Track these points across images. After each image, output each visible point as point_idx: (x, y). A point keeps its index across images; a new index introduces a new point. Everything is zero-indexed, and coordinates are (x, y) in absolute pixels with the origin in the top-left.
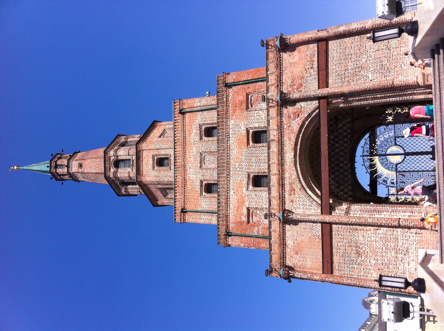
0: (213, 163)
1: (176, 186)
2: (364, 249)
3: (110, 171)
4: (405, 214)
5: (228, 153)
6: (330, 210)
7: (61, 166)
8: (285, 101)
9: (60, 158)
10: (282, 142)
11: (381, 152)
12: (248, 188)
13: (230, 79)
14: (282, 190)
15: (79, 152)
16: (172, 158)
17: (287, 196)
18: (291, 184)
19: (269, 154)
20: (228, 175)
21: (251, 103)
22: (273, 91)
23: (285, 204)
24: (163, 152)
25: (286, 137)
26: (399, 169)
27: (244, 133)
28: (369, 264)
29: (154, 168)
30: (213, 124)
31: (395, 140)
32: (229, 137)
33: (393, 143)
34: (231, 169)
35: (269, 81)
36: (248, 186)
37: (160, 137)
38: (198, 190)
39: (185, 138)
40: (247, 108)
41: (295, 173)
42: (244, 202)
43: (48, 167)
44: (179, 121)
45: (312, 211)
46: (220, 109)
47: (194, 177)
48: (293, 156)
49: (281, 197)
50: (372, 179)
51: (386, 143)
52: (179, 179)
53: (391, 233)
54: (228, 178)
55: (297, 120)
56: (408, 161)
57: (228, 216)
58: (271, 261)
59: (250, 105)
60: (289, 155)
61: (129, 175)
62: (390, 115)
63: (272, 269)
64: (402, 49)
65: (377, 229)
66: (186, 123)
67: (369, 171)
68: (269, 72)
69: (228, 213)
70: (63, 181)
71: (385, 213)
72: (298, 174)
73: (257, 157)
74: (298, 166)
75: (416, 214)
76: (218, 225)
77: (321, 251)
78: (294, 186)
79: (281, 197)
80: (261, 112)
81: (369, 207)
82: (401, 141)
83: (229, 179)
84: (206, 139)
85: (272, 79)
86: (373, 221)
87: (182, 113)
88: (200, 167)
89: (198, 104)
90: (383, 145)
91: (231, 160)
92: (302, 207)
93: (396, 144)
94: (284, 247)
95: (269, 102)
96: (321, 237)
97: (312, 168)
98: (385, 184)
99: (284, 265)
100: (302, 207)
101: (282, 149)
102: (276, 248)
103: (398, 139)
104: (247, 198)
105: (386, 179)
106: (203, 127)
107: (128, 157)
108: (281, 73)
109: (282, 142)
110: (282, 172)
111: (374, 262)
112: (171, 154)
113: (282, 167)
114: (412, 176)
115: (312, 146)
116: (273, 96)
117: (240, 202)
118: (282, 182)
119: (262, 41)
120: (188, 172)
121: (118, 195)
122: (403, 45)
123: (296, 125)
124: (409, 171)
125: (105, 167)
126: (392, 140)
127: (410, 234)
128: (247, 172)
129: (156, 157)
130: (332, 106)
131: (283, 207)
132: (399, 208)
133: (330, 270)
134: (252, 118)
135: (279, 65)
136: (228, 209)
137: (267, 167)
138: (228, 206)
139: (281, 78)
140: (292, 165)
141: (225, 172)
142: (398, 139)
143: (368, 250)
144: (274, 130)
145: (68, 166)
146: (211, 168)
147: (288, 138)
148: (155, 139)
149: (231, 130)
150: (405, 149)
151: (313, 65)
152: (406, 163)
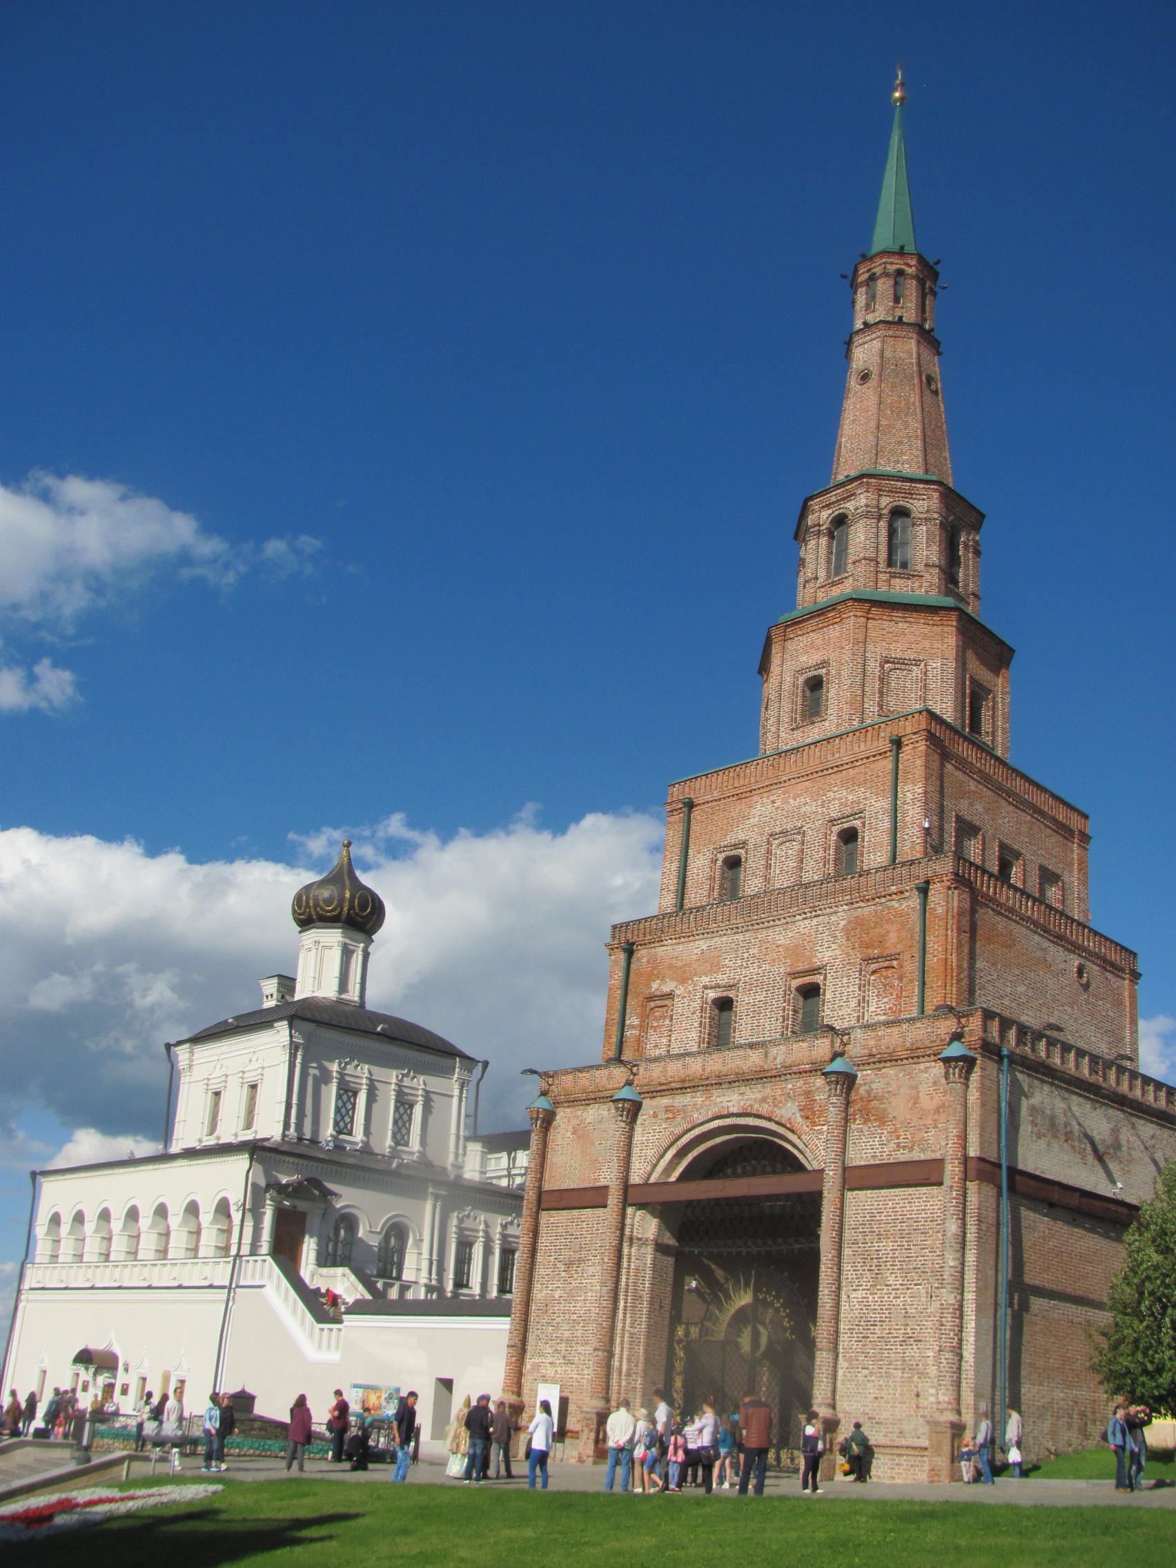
4: (625, 1361)
17: (665, 1101)
18: (684, 1110)
29: (800, 672)
38: (730, 839)
39: (839, 768)
40: (868, 960)
42: (683, 981)
58: (566, 1072)
60: (731, 1100)
64: (899, 1372)
66: (873, 766)
71: (628, 1321)
80: (853, 1003)
96: (598, 1184)
106: (857, 823)
111: (557, 1296)
112: (827, 723)
123: (790, 1111)
135: (915, 1054)
140: (715, 1110)
146: (768, 867)
151: (904, 1148)
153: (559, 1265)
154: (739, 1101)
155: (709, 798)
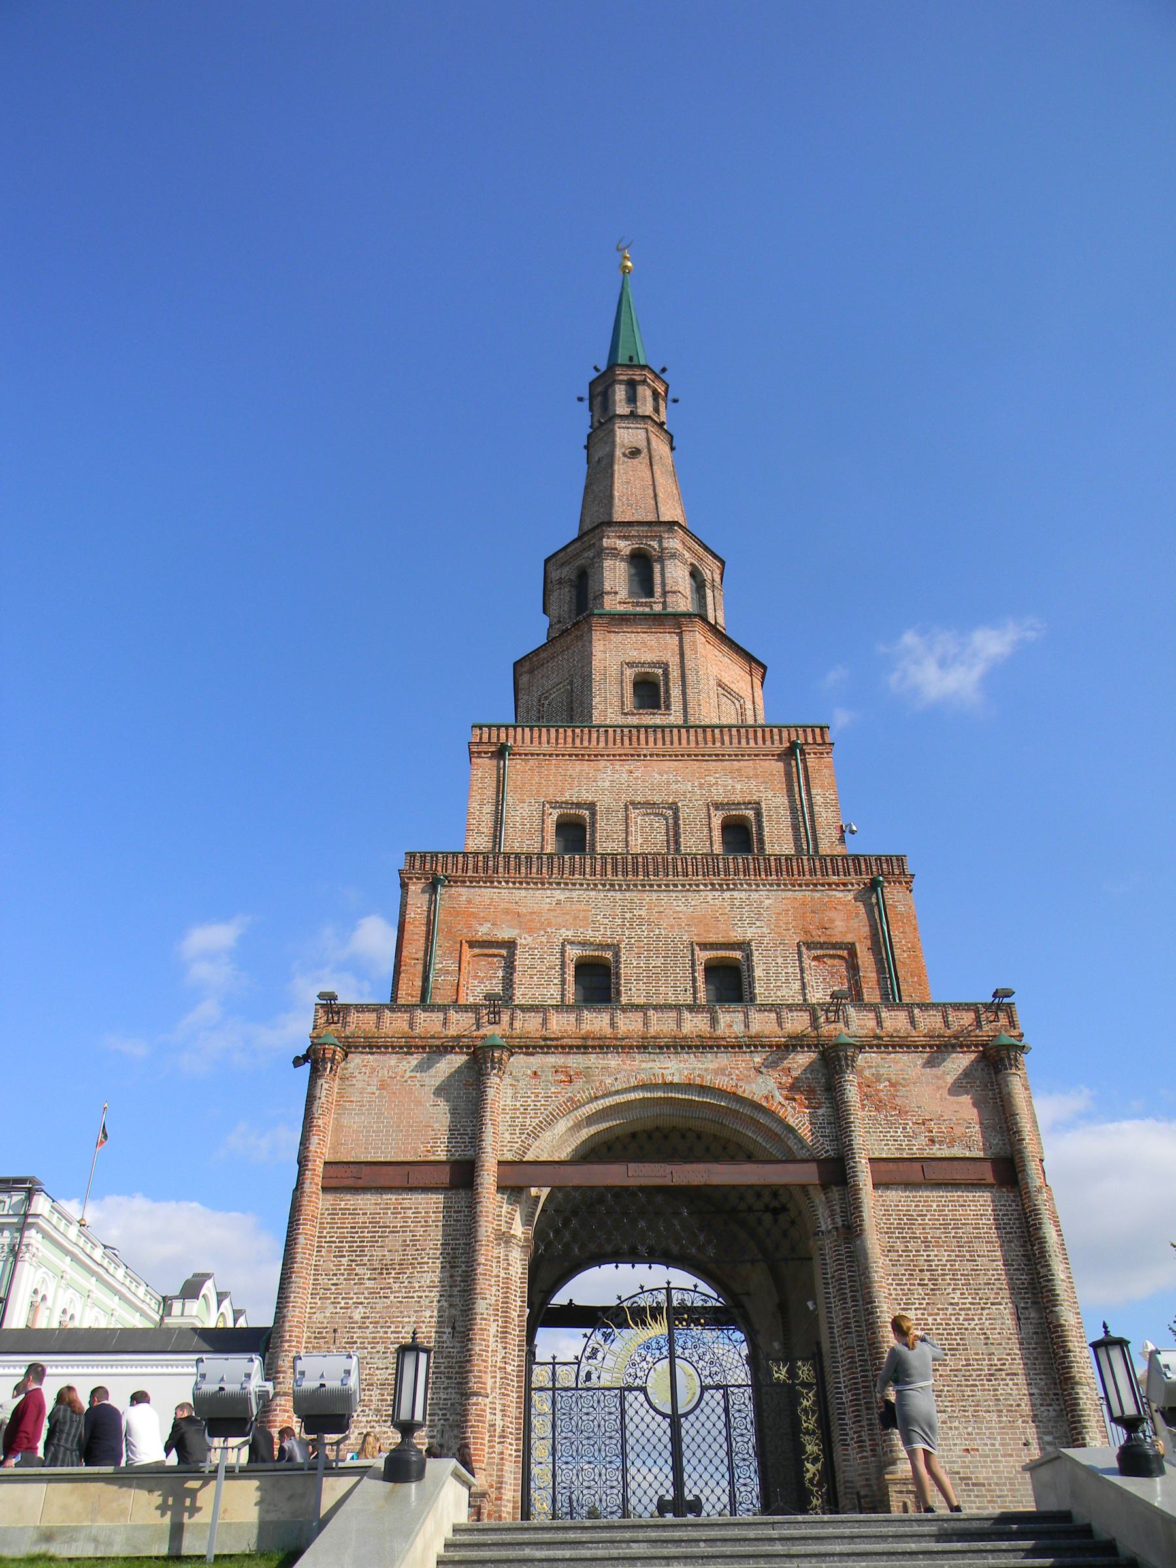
0: (646, 840)
1: (578, 731)
2: (396, 1286)
3: (619, 537)
5: (675, 886)
6: (512, 1190)
7: (632, 399)
8: (832, 1061)
9: (656, 395)
10: (711, 1047)
11: (681, 1342)
12: (572, 943)
13: (893, 894)
14: (571, 1047)
15: (672, 449)
16: (658, 720)
17: (552, 1060)
18: (586, 1073)
19: (677, 1008)
20: (612, 885)
21: (824, 956)
22: (862, 1023)
23: (527, 1054)
24: (675, 692)
25: (726, 1062)
26: (630, 1397)
27: (736, 935)
28: (351, 1302)
29: (630, 665)
30: (761, 841)
31: (717, 1387)
32: (723, 890)
33: (708, 1381)
34: (628, 894)
35: (892, 1013)
36: (580, 943)
37: (719, 684)
38: (566, 797)
39: (720, 758)
40: (809, 946)
41: (619, 1086)
42: (530, 931)
43: (631, 359)
44: (768, 743)
45: (507, 1135)
46: (806, 862)
47: (604, 784)
48: (669, 1079)
49: (549, 1043)
50: (600, 1314)
51: (707, 1358)
52: (597, 743)
53: (442, 1369)
54: (604, 885)
55: (777, 1094)
56: (653, 1426)
57: (492, 882)
59: (819, 952)
60: (675, 1068)
61: (608, 593)
62: (792, 1373)
63: (338, 1013)
65: (454, 1328)
66: (762, 763)
67: (625, 1304)
68: (916, 1011)
69: (500, 882)
70: (586, 403)
72: (617, 1092)
73: (666, 970)
74: (639, 1095)
75: (498, 1448)
76: (465, 855)
77: (388, 1159)
78: (579, 1083)
79: (549, 1043)
80: (797, 985)
81: (519, 1303)
82: (713, 1404)
83: (600, 887)
84: (717, 822)
85: (895, 1022)
86: (479, 1317)
87: (790, 753)
88: (632, 803)
89: (818, 800)
90: (701, 1351)
91: (654, 896)
92: (518, 1104)
93: (704, 1388)
94: (401, 1047)
95: (827, 1011)
96: (432, 1158)
97: (634, 1135)
98: (587, 1354)
99: (349, 1047)
100: (518, 1104)
101: (690, 1047)
102: (395, 1024)
103: (718, 1395)
104: (544, 939)
105: (600, 1356)
107: (658, 589)
108: (916, 1047)
109: (711, 1047)
110: (623, 1047)
111: (357, 1317)
112: (672, 718)
113: (638, 1047)
114: (611, 1438)
115: (699, 1137)
116: (847, 1024)
117: (532, 920)
118: (594, 1047)
119: (1009, 994)
120: (617, 767)
121: (547, 561)
122: (1004, 1419)
124: (623, 1427)
125: (630, 524)
126: (717, 1378)
127: (439, 1428)
128: (620, 942)
129: (660, 671)
130: (819, 1198)
131: (520, 1047)
132: (515, 1395)
133: (334, 1183)
134: (780, 960)
136: (511, 885)
137: (636, 1001)
138: (521, 883)
139: (900, 1046)
140: (643, 1077)
141: (620, 877)
142: (718, 1395)
143: (392, 1298)
144: (747, 1026)
145: (633, 416)
147: (722, 1066)
148: (714, 671)
149: (743, 895)
150: (691, 1417)
151: (941, 1143)
152: (648, 1419)
153: (359, 1270)
154: (680, 1071)
155: (529, 750)
